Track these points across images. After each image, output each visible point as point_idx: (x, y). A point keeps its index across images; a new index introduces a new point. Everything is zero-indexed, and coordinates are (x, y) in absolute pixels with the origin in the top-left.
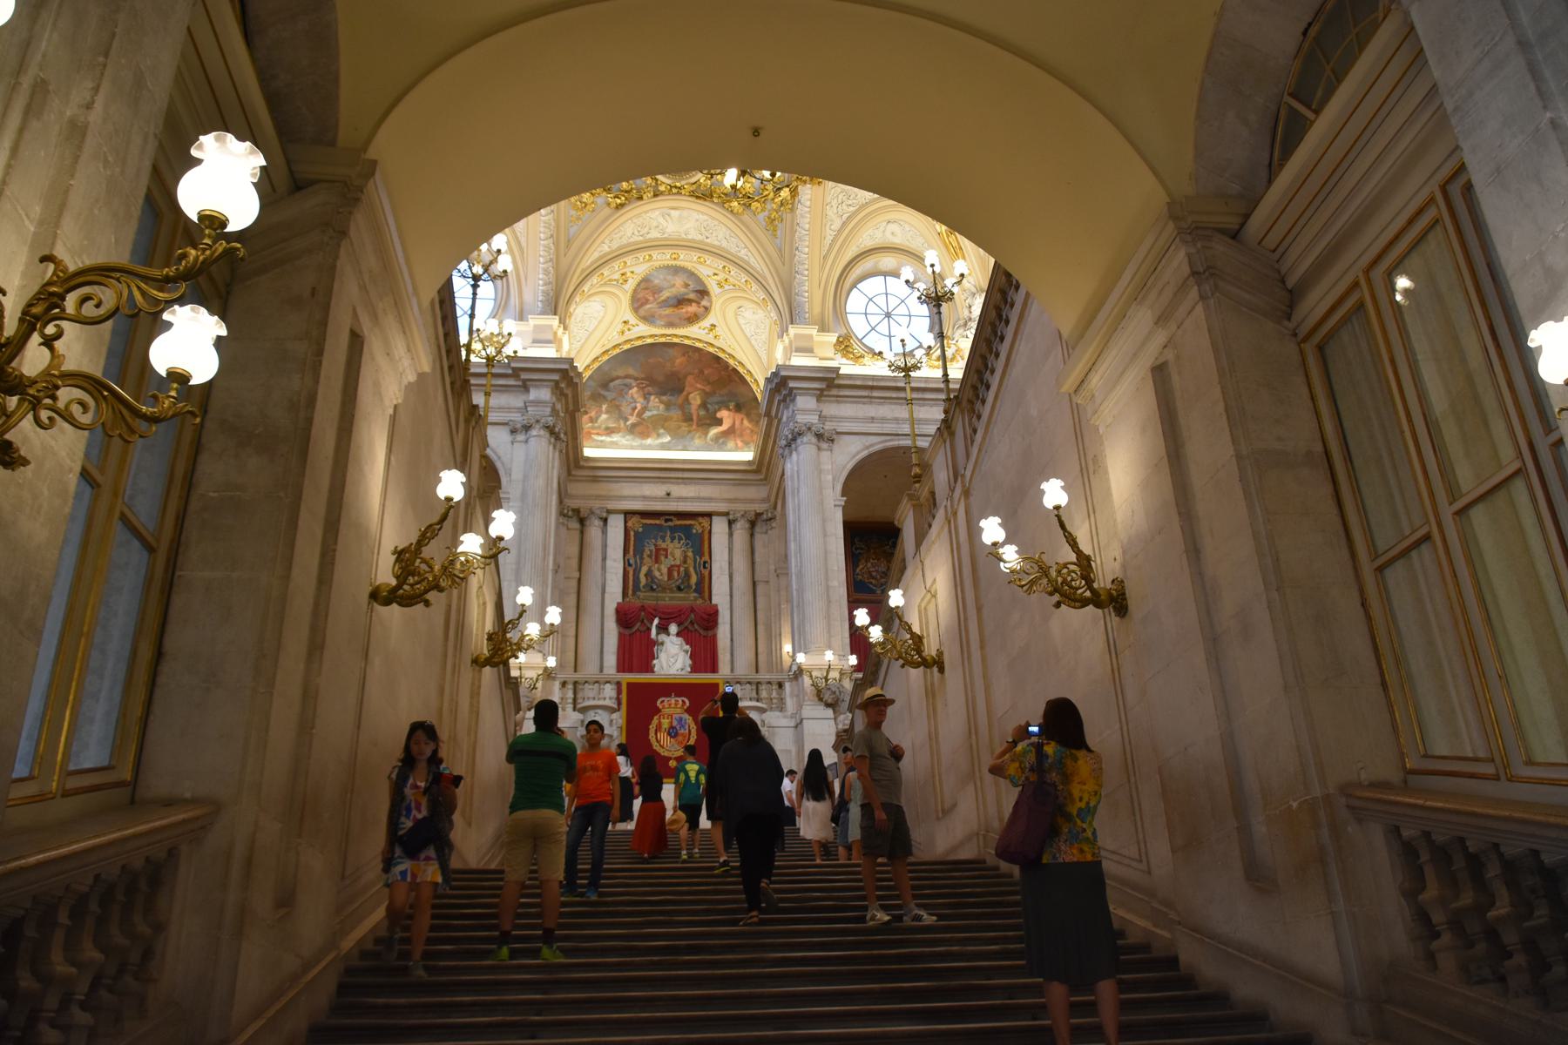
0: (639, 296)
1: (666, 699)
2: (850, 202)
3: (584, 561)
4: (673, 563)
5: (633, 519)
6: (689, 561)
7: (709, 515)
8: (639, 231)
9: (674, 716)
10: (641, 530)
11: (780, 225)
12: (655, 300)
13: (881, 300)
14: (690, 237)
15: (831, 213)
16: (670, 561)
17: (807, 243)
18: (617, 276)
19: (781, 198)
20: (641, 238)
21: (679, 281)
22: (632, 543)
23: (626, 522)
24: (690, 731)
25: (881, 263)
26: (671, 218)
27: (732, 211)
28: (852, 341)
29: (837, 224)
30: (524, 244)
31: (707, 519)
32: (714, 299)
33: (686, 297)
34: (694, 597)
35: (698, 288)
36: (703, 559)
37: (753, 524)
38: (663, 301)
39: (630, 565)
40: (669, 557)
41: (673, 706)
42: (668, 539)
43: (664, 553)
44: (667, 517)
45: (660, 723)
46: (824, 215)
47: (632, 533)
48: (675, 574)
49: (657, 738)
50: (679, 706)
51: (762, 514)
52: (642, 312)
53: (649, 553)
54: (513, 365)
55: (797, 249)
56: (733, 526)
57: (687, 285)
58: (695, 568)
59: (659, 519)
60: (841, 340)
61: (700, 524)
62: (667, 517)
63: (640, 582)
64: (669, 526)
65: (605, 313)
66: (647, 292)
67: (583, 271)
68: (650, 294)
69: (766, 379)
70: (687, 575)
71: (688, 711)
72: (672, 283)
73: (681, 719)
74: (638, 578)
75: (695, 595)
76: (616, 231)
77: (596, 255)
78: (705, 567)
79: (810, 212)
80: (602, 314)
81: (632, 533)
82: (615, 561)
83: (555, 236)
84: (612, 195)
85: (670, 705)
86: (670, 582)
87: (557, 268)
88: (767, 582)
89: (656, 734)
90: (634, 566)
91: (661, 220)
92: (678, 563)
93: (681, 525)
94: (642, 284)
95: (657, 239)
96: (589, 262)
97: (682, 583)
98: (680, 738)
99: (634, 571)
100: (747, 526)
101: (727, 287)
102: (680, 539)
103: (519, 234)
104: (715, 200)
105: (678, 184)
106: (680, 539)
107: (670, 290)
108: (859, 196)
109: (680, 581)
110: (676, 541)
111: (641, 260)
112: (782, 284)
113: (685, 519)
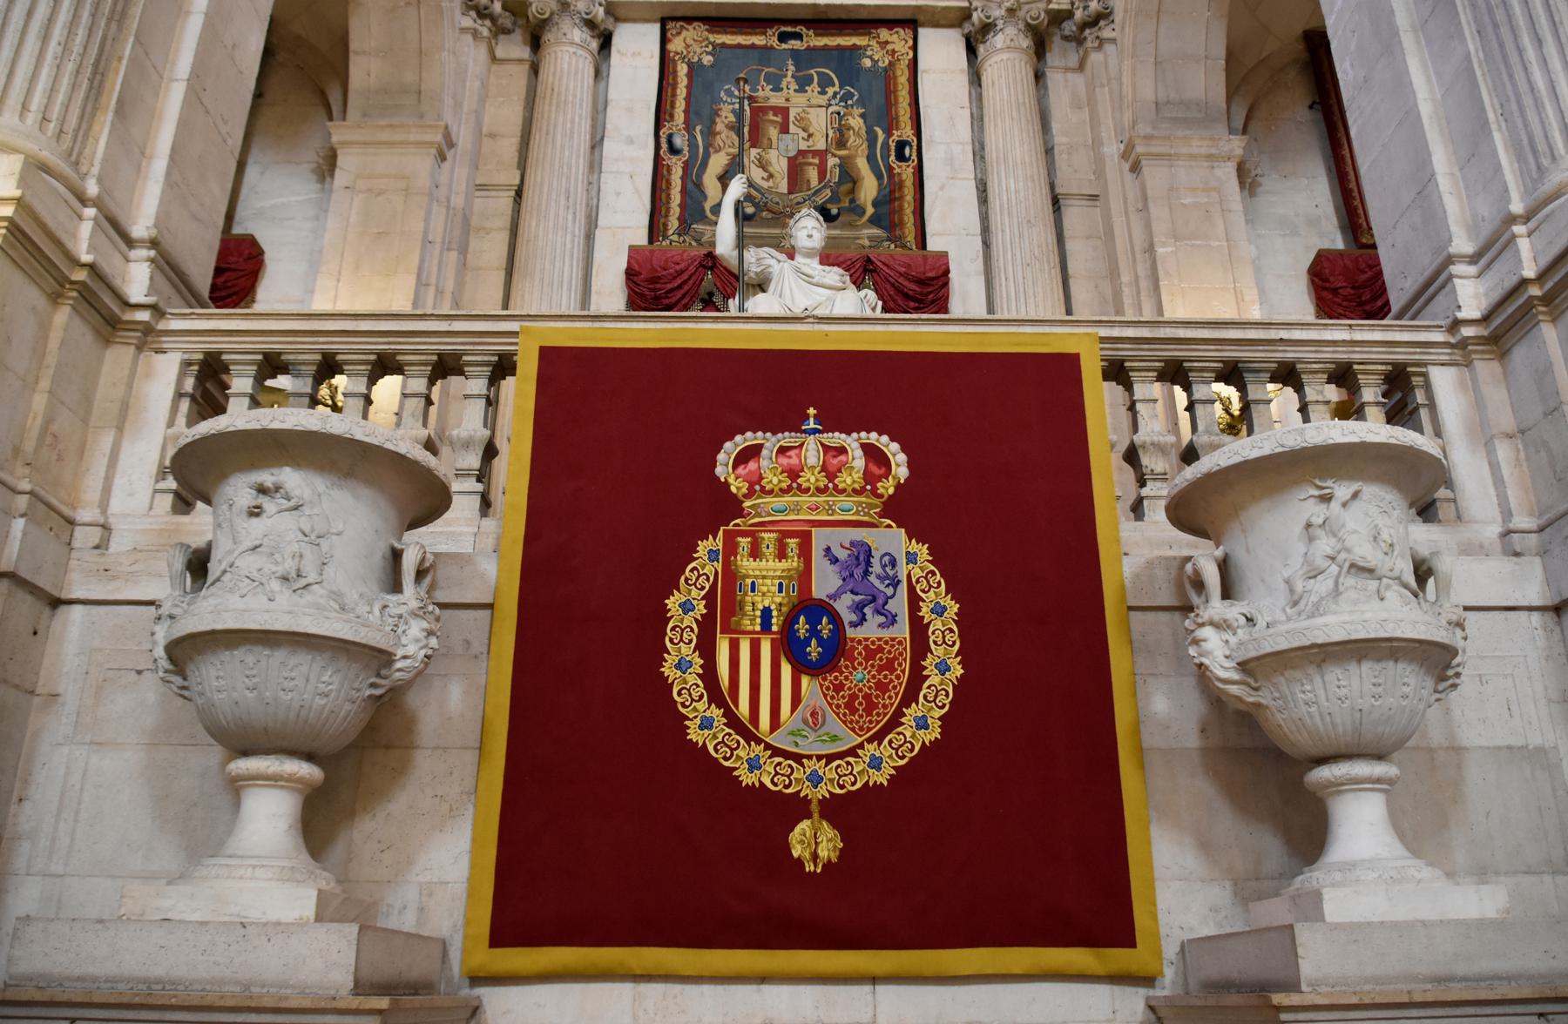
1: (770, 442)
3: (537, 138)
4: (803, 146)
5: (684, 33)
6: (852, 140)
7: (910, 22)
9: (820, 538)
10: (707, 60)
16: (795, 142)
22: (682, 92)
23: (664, 41)
24: (919, 629)
31: (903, 33)
34: (871, 239)
36: (895, 137)
37: (1040, 48)
39: (674, 150)
40: (792, 128)
41: (810, 478)
42: (789, 81)
43: (779, 119)
44: (789, 29)
45: (730, 576)
47: (682, 70)
48: (812, 174)
49: (709, 675)
50: (846, 480)
51: (1069, 14)
53: (732, 118)
56: (981, 49)
58: (871, 159)
59: (764, 33)
61: (884, 44)
62: (789, 29)
63: (705, 197)
64: (795, 53)
70: (849, 177)
71: (899, 509)
73: (863, 555)
74: (699, 186)
75: (876, 231)
78: (901, 157)
81: (682, 70)
82: (630, 141)
85: (794, 474)
86: (798, 197)
88: (1094, 197)
89: (706, 648)
90: (686, 149)
92: (821, 145)
93: (825, 48)
97: (835, 198)
98: (860, 677)
99: (687, 167)
100: (1026, 42)
102: (825, 83)
106: (825, 83)
109: (828, 193)
110: (815, 87)
113: (841, 35)
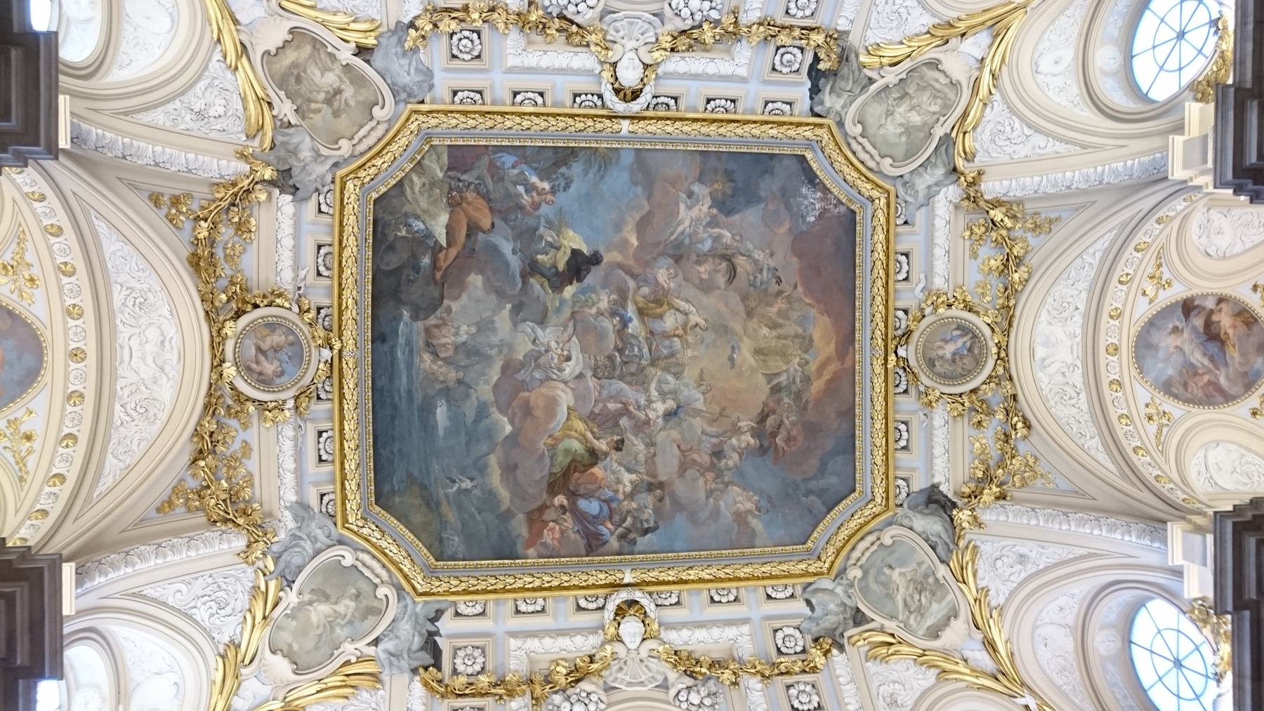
0: (1200, 394)
2: (1008, 129)
8: (1070, 398)
11: (1043, 216)
12: (1209, 371)
13: (1161, 53)
14: (1079, 331)
15: (1023, 151)
17: (1060, 175)
18: (1152, 428)
19: (1006, 219)
20: (1083, 396)
21: (1167, 342)
25: (1107, 68)
26: (1049, 357)
27: (1027, 281)
28: (1201, 78)
29: (1040, 140)
30: (1084, 551)
32: (1194, 292)
33: (1201, 330)
35: (1179, 312)
38: (1212, 359)
46: (1027, 159)
52: (1233, 391)
54: (1230, 608)
55: (1069, 187)
57: (1176, 330)
60: (1200, 96)
65: (1231, 442)
66: (1191, 383)
67: (1123, 476)
68: (1197, 378)
69: (1251, 202)
72: (1172, 350)
76: (1067, 428)
77: (1102, 457)
79: (1017, 179)
80: (1234, 447)
83: (1064, 510)
84: (1013, 433)
87: (1109, 512)
91: (1053, 369)
94: (1175, 391)
95: (1085, 375)
96: (1112, 468)
101: (1166, 275)
103: (1071, 556)
104: (1012, 302)
105: (995, 350)
107: (1187, 352)
108: (999, 119)
111: (1120, 394)
112: (1121, 200)
